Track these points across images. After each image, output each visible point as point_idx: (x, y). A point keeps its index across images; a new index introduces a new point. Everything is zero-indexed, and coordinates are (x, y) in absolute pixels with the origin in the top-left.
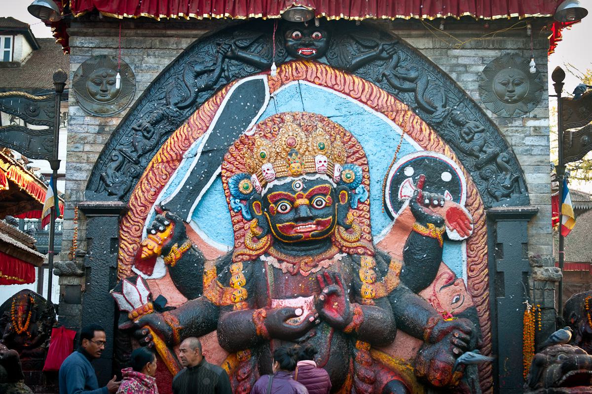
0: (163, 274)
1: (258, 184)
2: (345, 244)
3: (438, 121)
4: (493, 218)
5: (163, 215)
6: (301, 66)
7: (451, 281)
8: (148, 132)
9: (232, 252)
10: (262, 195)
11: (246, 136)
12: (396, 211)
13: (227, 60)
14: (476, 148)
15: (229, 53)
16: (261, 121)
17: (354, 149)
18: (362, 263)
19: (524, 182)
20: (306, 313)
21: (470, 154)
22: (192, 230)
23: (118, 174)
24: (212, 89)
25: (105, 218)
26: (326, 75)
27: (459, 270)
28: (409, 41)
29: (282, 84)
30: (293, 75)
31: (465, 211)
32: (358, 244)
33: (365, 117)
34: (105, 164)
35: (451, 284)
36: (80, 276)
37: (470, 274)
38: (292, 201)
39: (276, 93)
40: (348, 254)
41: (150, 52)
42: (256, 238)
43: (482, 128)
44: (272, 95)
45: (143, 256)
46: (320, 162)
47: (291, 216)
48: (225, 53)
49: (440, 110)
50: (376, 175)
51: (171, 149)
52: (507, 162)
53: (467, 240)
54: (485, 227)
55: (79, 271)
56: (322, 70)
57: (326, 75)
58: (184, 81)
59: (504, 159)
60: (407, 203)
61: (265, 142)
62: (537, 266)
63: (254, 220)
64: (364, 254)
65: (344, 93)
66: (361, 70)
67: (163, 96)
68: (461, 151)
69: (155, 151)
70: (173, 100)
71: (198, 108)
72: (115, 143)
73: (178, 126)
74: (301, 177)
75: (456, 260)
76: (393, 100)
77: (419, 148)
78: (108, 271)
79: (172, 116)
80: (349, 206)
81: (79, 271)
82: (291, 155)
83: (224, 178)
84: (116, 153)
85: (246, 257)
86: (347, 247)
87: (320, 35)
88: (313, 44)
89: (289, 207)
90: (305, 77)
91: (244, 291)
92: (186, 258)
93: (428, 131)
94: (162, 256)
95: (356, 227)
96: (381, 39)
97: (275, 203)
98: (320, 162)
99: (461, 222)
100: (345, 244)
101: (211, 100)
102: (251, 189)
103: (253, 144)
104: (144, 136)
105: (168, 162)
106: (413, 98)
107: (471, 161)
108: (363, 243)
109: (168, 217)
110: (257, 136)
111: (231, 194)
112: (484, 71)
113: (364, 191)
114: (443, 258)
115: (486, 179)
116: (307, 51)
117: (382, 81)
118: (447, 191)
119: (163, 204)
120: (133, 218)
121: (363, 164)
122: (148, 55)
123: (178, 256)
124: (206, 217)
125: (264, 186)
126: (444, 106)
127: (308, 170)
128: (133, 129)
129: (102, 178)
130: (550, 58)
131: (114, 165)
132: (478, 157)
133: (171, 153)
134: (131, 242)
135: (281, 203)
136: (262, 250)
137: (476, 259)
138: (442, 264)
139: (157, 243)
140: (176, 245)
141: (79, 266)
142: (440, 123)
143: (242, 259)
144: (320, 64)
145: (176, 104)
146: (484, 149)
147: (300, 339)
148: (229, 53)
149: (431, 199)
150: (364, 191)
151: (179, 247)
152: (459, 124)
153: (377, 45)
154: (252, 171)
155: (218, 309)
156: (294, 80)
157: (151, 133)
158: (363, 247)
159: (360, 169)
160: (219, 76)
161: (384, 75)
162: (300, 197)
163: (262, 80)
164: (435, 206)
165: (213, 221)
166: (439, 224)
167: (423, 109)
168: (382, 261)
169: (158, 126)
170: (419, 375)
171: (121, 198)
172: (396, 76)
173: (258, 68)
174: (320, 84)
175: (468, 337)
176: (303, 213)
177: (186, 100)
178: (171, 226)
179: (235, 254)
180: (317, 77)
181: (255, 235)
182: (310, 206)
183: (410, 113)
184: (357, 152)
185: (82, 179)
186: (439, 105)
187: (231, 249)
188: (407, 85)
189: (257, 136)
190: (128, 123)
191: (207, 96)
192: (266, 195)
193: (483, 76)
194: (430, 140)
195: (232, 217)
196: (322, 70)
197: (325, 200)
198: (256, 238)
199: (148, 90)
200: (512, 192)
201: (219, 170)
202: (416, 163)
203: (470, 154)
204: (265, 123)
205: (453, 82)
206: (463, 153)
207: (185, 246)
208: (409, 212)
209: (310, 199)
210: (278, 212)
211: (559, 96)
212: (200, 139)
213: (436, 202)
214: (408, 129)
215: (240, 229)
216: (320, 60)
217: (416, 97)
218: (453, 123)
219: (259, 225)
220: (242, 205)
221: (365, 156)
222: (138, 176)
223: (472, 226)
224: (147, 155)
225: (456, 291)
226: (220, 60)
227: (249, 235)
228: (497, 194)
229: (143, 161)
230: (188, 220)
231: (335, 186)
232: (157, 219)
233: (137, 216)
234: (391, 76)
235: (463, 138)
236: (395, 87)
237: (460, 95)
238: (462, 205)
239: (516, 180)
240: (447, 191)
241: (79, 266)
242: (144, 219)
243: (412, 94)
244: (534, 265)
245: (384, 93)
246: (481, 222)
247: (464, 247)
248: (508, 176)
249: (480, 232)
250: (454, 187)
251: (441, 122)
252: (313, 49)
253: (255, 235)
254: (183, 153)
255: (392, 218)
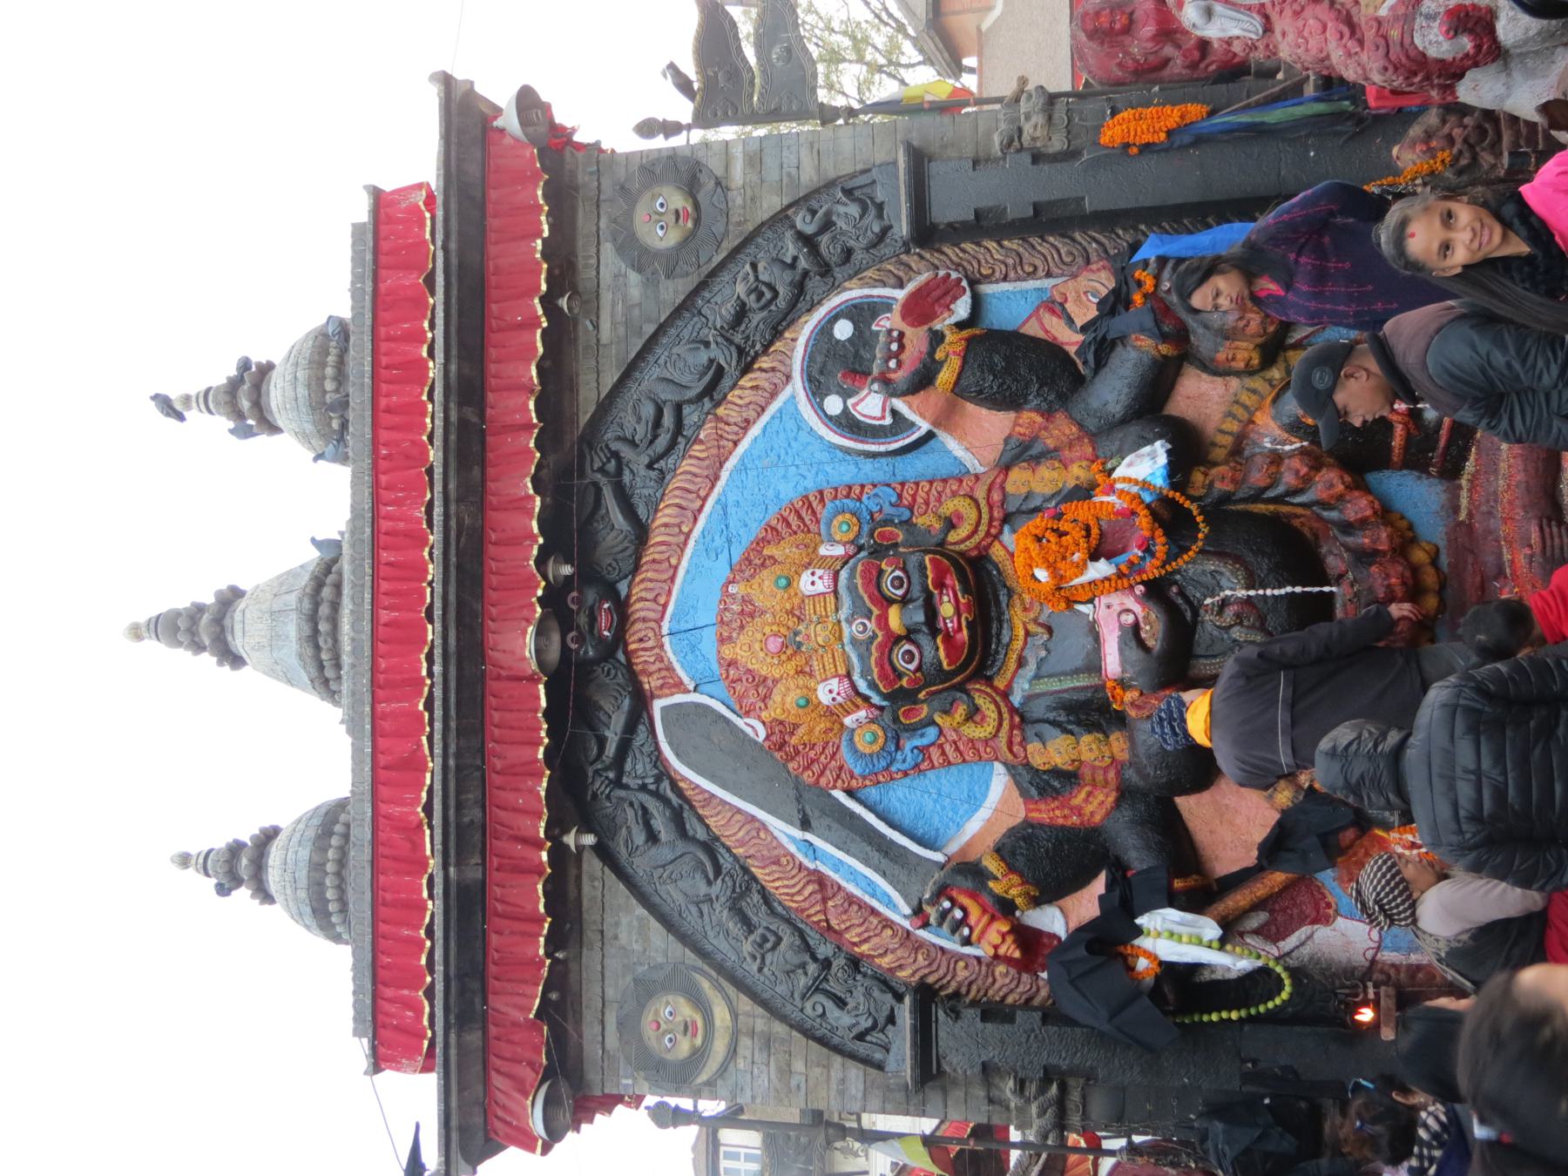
0: (1057, 912)
1: (862, 714)
2: (983, 528)
3: (735, 355)
4: (926, 234)
5: (932, 913)
6: (636, 631)
7: (1058, 308)
8: (765, 939)
9: (1005, 764)
10: (884, 703)
11: (767, 738)
12: (912, 425)
13: (625, 780)
14: (788, 276)
15: (611, 775)
16: (737, 708)
17: (793, 519)
18: (1024, 490)
19: (853, 176)
20: (1130, 603)
21: (800, 288)
22: (963, 850)
23: (851, 1004)
24: (681, 808)
25: (942, 1034)
26: (651, 580)
27: (1035, 294)
28: (584, 419)
29: (670, 669)
30: (652, 648)
31: (911, 287)
32: (983, 503)
33: (731, 501)
34: (834, 1030)
35: (1064, 309)
36: (1063, 1089)
37: (1041, 273)
38: (898, 640)
39: (686, 680)
40: (1007, 519)
41: (608, 934)
42: (973, 713)
43: (748, 267)
44: (691, 687)
45: (1017, 954)
46: (813, 583)
47: (924, 640)
48: (611, 782)
49: (714, 352)
50: (845, 473)
51: (799, 892)
52: (814, 213)
53: (973, 283)
54: (946, 249)
55: (1054, 1089)
56: (646, 589)
57: (651, 580)
58: (663, 866)
59: (808, 218)
60: (899, 404)
61: (777, 697)
62: (1020, 137)
63: (938, 719)
64: (1003, 488)
65: (686, 543)
66: (642, 511)
67: (694, 909)
68: (794, 305)
69: (802, 926)
70: (703, 888)
71: (717, 839)
72: (789, 1007)
73: (754, 878)
74: (844, 624)
75: (1014, 302)
76: (697, 447)
77: (788, 390)
78: (1053, 1029)
79: (734, 891)
80: (908, 523)
81: (1054, 1089)
82: (799, 645)
83: (854, 783)
84: (808, 1005)
85: (1017, 739)
86: (990, 525)
87: (575, 594)
88: (592, 608)
89: (907, 647)
90: (653, 624)
91: (1086, 739)
92: (1020, 862)
93: (758, 374)
94: (1018, 913)
95: (949, 507)
96: (582, 474)
97: (900, 676)
98: (813, 583)
99: (936, 294)
100: (983, 528)
101: (700, 812)
102: (874, 727)
103: (781, 723)
104: (774, 948)
105: (825, 900)
106: (693, 407)
107: (814, 283)
108: (980, 494)
109: (935, 900)
110: (764, 714)
111: (887, 768)
112: (640, 270)
113: (876, 495)
114: (1010, 327)
115: (848, 253)
116: (603, 620)
117: (661, 471)
118: (874, 328)
119: (907, 911)
120: (941, 972)
121: (822, 500)
122: (616, 938)
123: (1015, 879)
124: (936, 821)
125: (866, 699)
126: (707, 344)
127: (831, 607)
128: (760, 970)
129: (861, 1037)
130: (622, 148)
131: (833, 1012)
132: (805, 274)
133: (806, 893)
134: (990, 980)
135: (900, 663)
136: (1002, 704)
137: (1010, 261)
138: (1022, 331)
139: (989, 924)
140: (991, 884)
141: (1042, 1090)
142: (741, 351)
143: (1020, 744)
144: (629, 596)
145: (709, 883)
146: (789, 260)
147: (1188, 615)
148: (611, 775)
149: (890, 355)
150: (876, 495)
151: (996, 878)
152: (742, 313)
153: (596, 485)
154: (836, 727)
155: (1125, 794)
156: (662, 646)
157: (769, 935)
158: (989, 490)
159: (829, 505)
160: (657, 795)
161: (650, 466)
162: (883, 621)
163: (664, 709)
164: (902, 347)
165: (943, 808)
166: (937, 338)
167: (713, 387)
168: (1021, 453)
169: (755, 919)
170: (1256, 362)
171: (899, 998)
172: (651, 442)
173: (640, 716)
174: (670, 592)
175: (1170, 265)
176: (920, 617)
177: (702, 864)
178: (954, 894)
179: (1010, 756)
180: (655, 600)
181: (969, 718)
182: (904, 601)
183: (721, 411)
184: (798, 513)
185: (861, 1079)
186: (703, 356)
187: (999, 767)
188: (668, 420)
189: (764, 714)
190: (749, 981)
191: (695, 820)
192: (885, 697)
193: (649, 271)
194: (773, 369)
195: (933, 767)
196: (646, 589)
197: (891, 573)
198: (973, 713)
199: (684, 938)
200: (872, 199)
201: (839, 795)
202: (817, 390)
203: (800, 288)
204: (740, 699)
205: (661, 329)
206: (797, 301)
207: (992, 865)
208: (916, 400)
209: (890, 602)
210: (919, 668)
211: (689, 127)
212: (776, 833)
213: (894, 347)
214: (754, 414)
215: (957, 749)
216: (623, 594)
217: (690, 402)
218: (739, 324)
219: (946, 712)
220: (908, 745)
221: (805, 499)
222: (855, 963)
223: (942, 273)
224: (811, 943)
225: (1078, 300)
226: (622, 793)
227: (971, 731)
228: (876, 229)
229: (824, 951)
230: (939, 857)
231: (863, 554)
232: (940, 924)
233: (934, 967)
234: (650, 452)
235: (770, 302)
236: (673, 444)
237: (687, 315)
238: (900, 294)
239: (848, 192)
240: (874, 328)
241: (1042, 1090)
242: (942, 948)
243: (686, 410)
244: (1016, 143)
245: (686, 465)
246: (935, 258)
247: (987, 289)
248: (841, 209)
249: (954, 258)
250: (862, 314)
251: (738, 347)
252: (600, 608)
253: (969, 718)
254: (807, 869)
255: (930, 435)
